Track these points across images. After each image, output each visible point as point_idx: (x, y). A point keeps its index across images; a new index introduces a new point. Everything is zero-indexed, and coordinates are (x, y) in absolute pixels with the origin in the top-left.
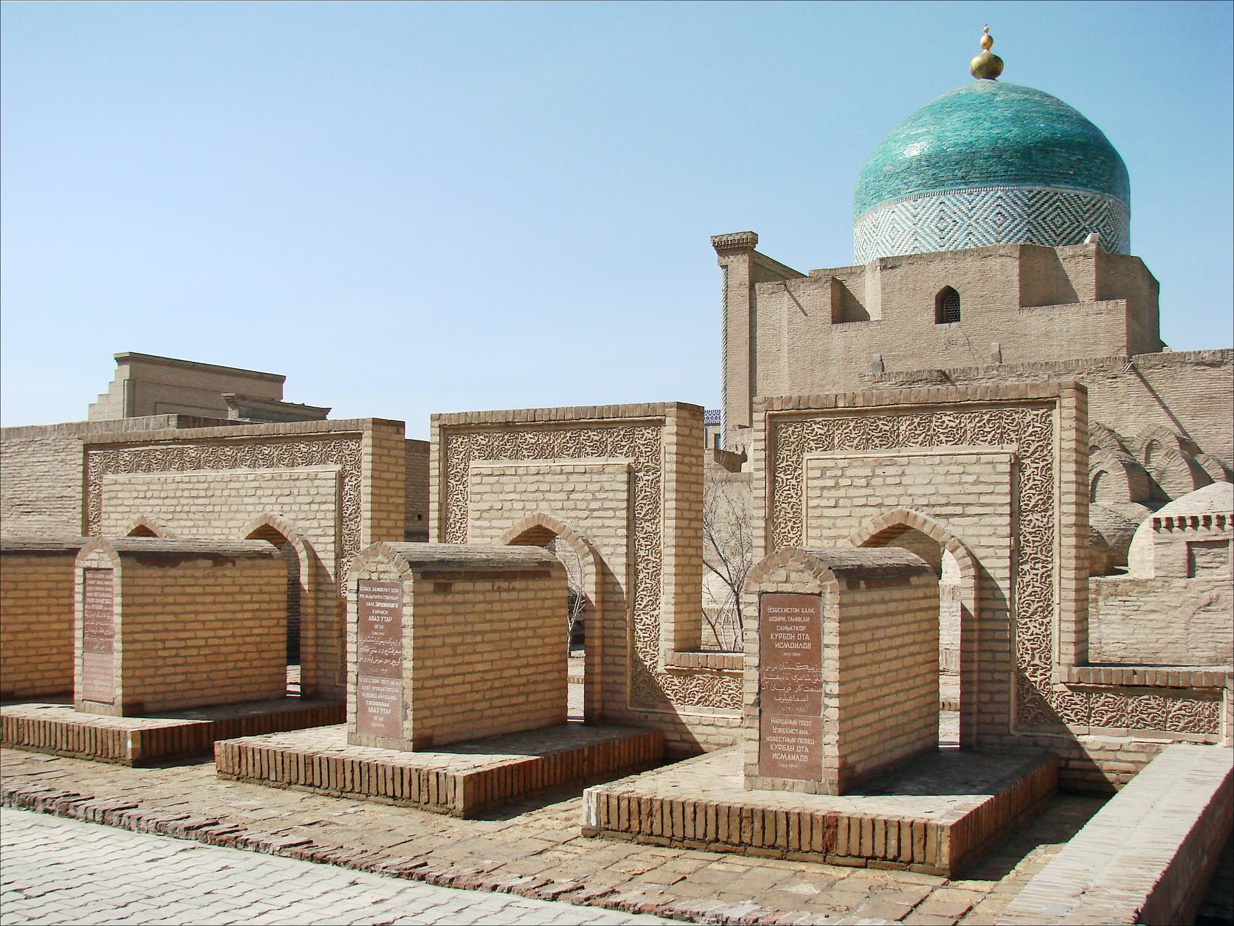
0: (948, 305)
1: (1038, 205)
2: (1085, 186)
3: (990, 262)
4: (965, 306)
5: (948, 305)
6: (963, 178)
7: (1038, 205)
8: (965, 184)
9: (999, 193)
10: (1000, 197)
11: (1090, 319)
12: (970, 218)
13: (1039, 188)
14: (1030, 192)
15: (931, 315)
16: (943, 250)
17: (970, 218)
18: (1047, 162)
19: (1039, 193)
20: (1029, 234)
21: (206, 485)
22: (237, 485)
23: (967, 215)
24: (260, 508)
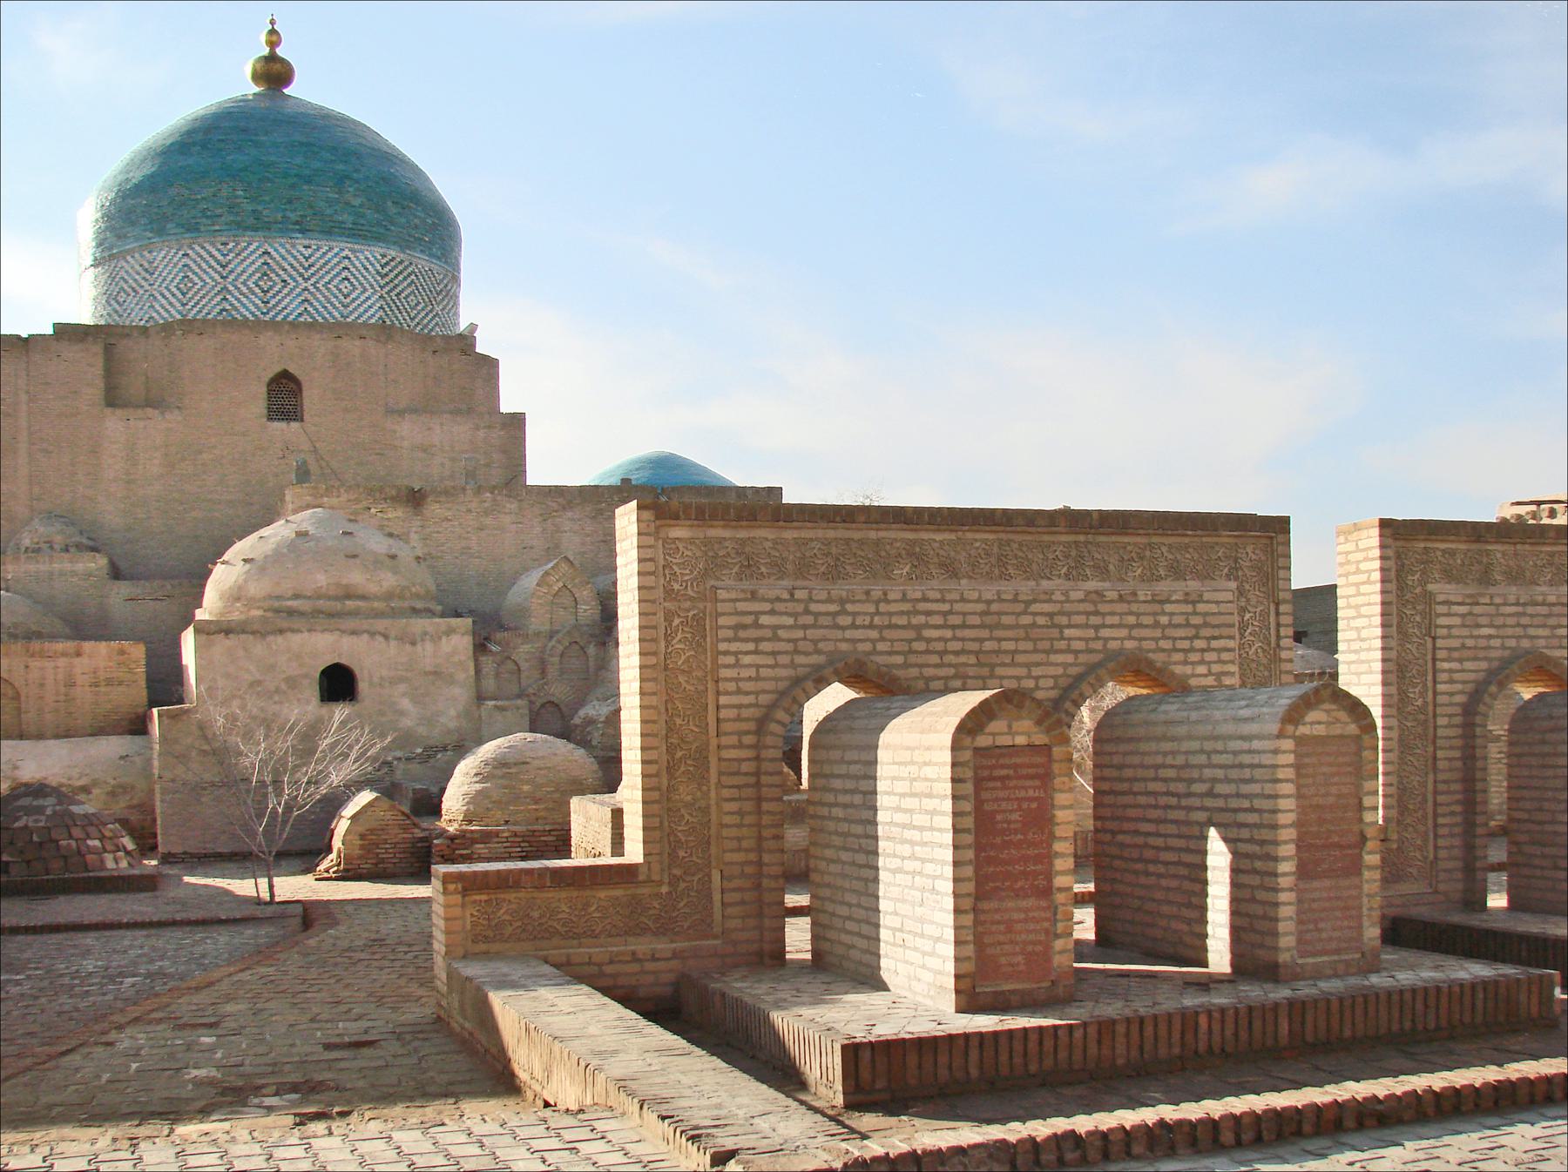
0: (285, 395)
1: (392, 275)
2: (439, 258)
3: (345, 343)
4: (311, 399)
5: (285, 395)
6: (297, 223)
7: (392, 275)
8: (302, 231)
9: (346, 252)
10: (347, 257)
11: (481, 433)
12: (306, 280)
13: (394, 254)
14: (384, 256)
15: (260, 406)
16: (267, 318)
17: (306, 280)
18: (403, 220)
19: (393, 259)
20: (381, 313)
21: (980, 607)
22: (1047, 608)
23: (301, 275)
24: (1098, 645)
